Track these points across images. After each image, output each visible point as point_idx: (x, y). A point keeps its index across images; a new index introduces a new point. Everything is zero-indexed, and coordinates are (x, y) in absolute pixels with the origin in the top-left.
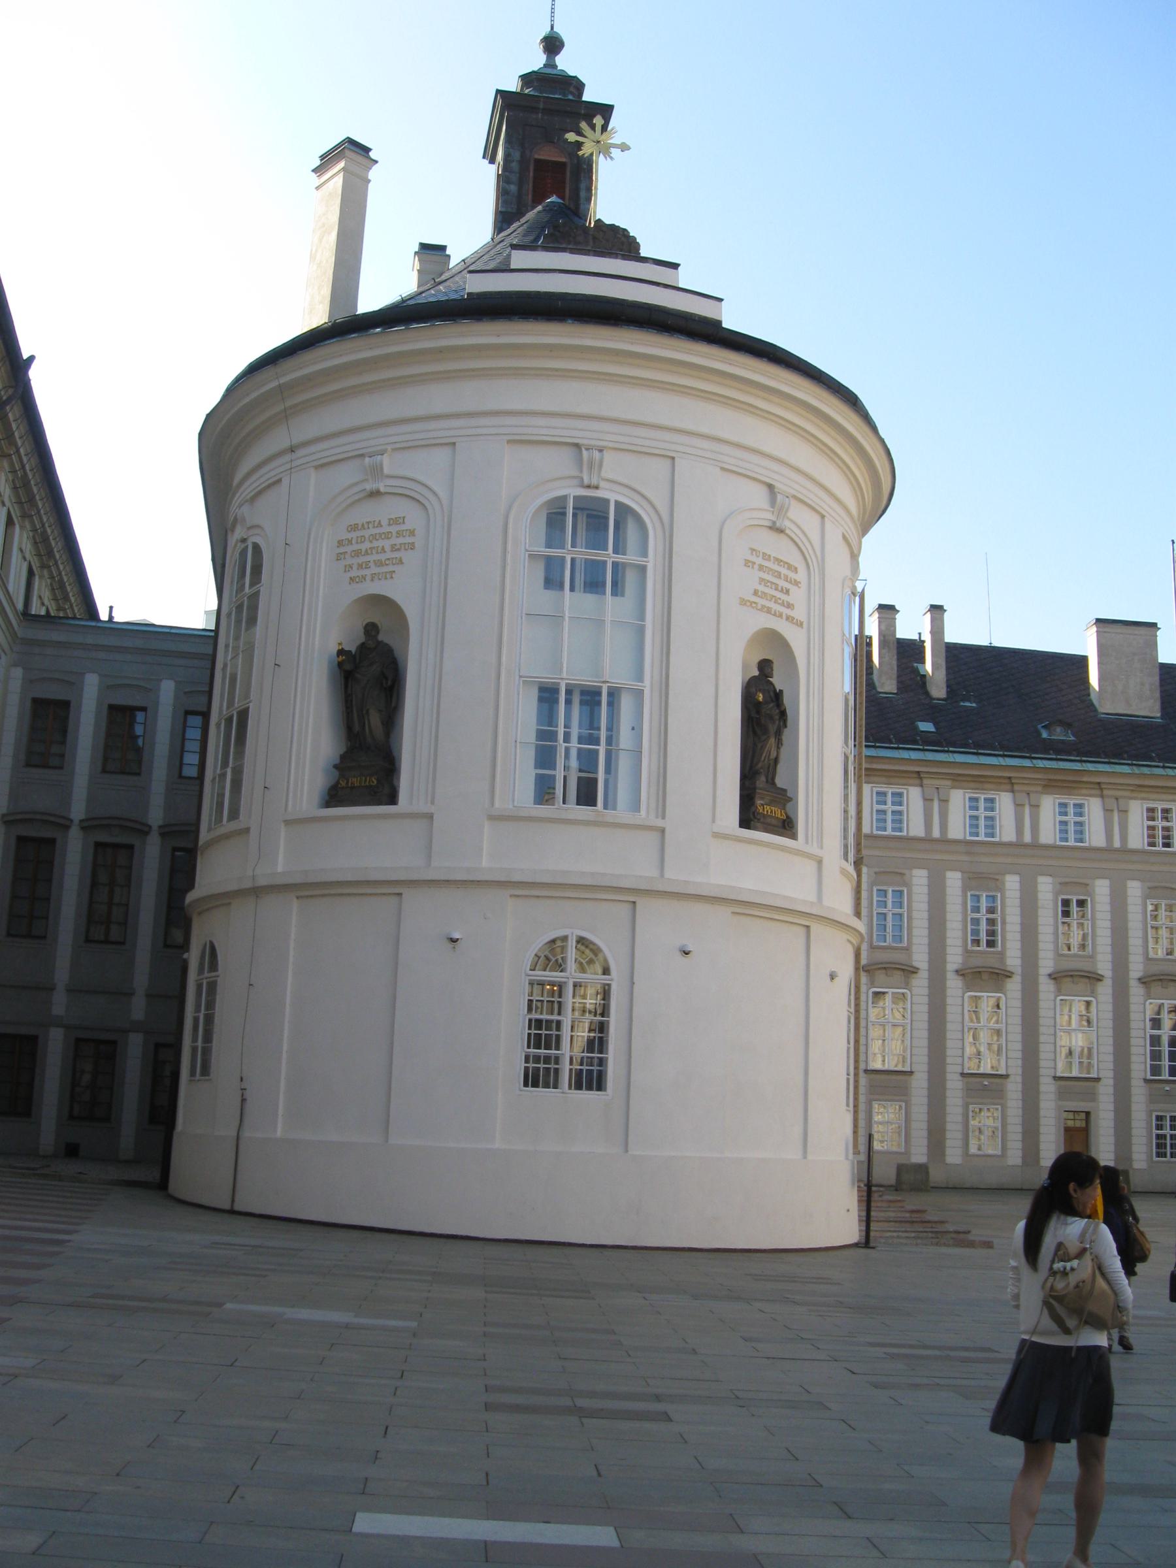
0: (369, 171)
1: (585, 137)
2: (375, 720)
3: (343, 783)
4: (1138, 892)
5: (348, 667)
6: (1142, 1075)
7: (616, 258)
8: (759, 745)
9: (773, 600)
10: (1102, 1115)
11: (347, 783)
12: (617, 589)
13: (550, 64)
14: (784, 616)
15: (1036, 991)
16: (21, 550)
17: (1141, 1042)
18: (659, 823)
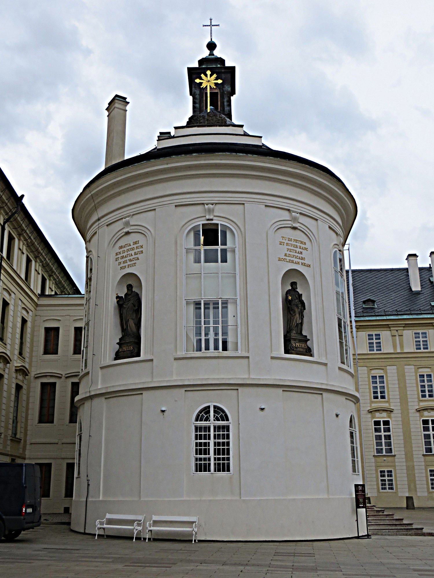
0: (126, 107)
1: (203, 80)
2: (132, 324)
3: (121, 350)
5: (121, 303)
7: (217, 126)
8: (292, 318)
9: (294, 257)
11: (122, 350)
13: (211, 54)
14: (300, 263)
16: (36, 270)
18: (246, 355)
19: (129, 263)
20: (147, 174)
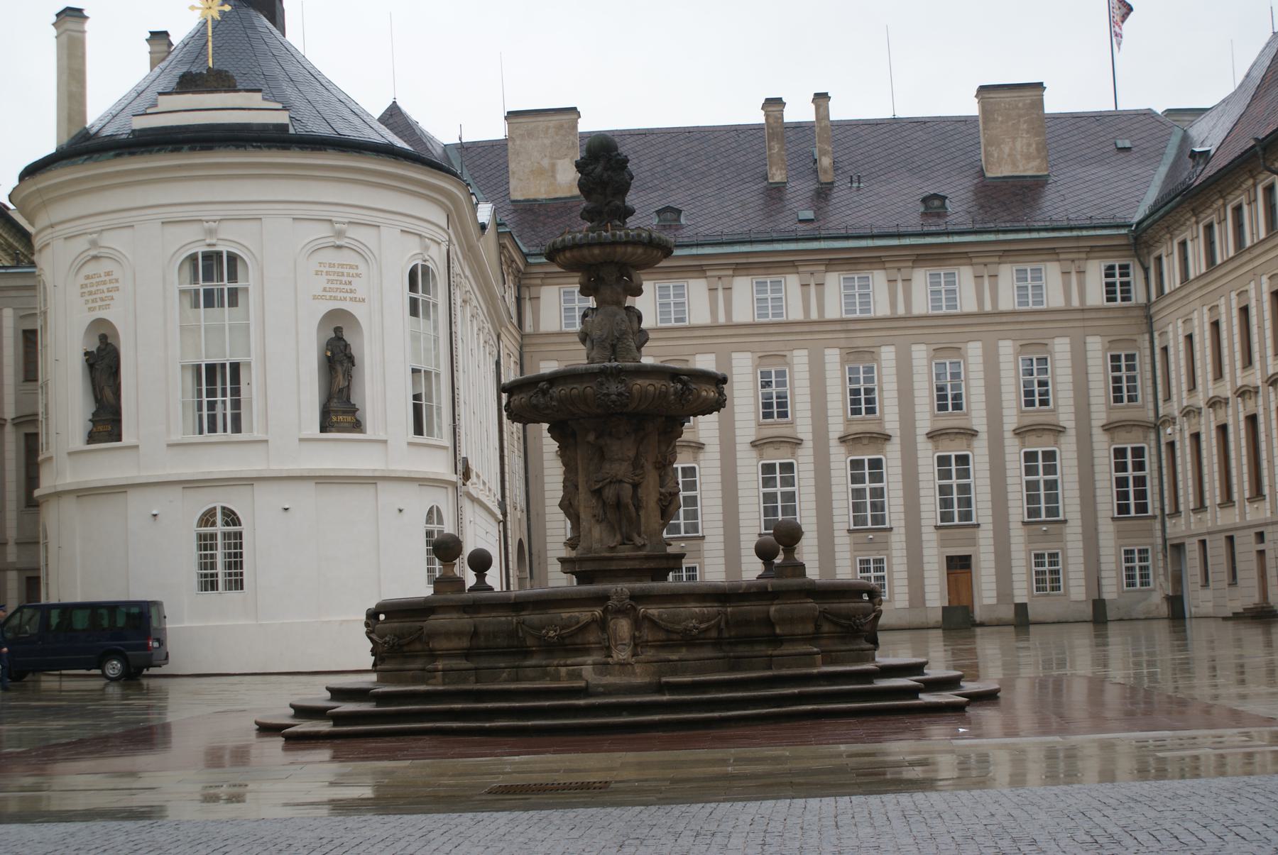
2: (108, 393)
4: (1010, 350)
5: (91, 362)
6: (1020, 518)
10: (982, 557)
12: (233, 302)
14: (348, 299)
15: (828, 462)
17: (1018, 488)
19: (100, 303)
20: (117, 174)
